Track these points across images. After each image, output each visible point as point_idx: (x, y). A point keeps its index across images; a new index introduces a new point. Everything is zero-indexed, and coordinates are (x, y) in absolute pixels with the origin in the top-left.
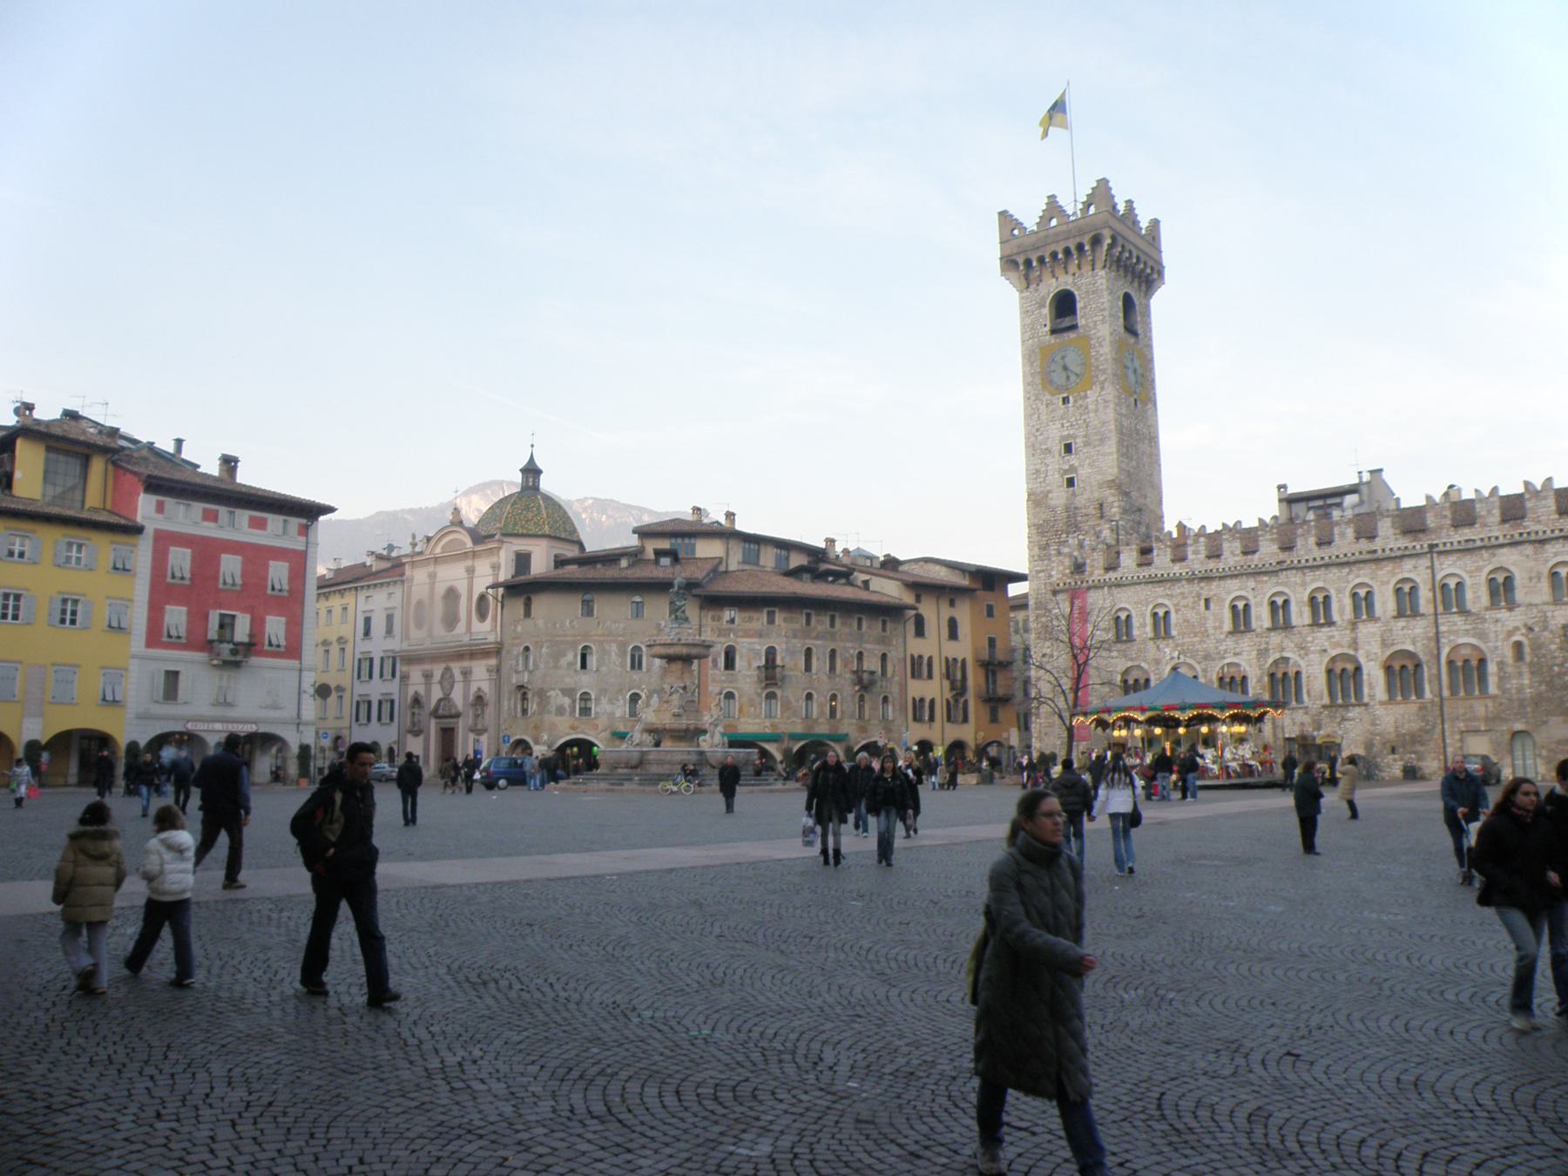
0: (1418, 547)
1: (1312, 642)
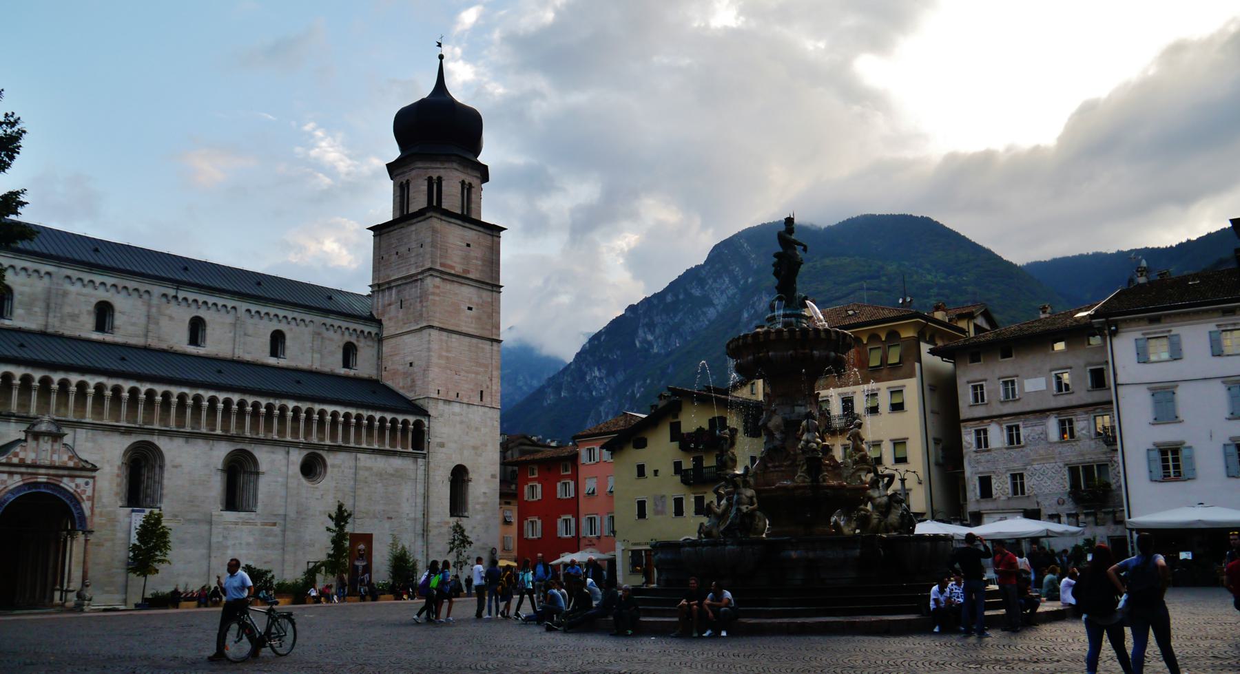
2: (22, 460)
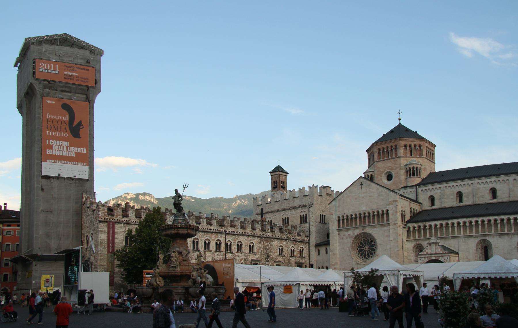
0: (222, 231)
1: (193, 256)
2: (427, 253)
